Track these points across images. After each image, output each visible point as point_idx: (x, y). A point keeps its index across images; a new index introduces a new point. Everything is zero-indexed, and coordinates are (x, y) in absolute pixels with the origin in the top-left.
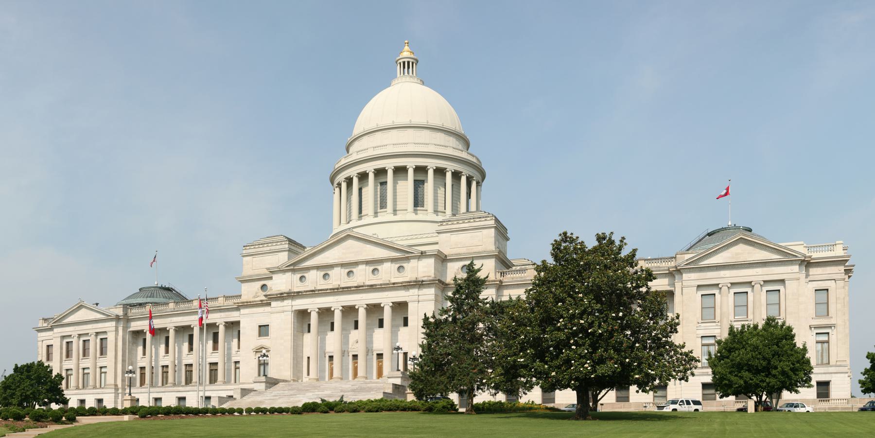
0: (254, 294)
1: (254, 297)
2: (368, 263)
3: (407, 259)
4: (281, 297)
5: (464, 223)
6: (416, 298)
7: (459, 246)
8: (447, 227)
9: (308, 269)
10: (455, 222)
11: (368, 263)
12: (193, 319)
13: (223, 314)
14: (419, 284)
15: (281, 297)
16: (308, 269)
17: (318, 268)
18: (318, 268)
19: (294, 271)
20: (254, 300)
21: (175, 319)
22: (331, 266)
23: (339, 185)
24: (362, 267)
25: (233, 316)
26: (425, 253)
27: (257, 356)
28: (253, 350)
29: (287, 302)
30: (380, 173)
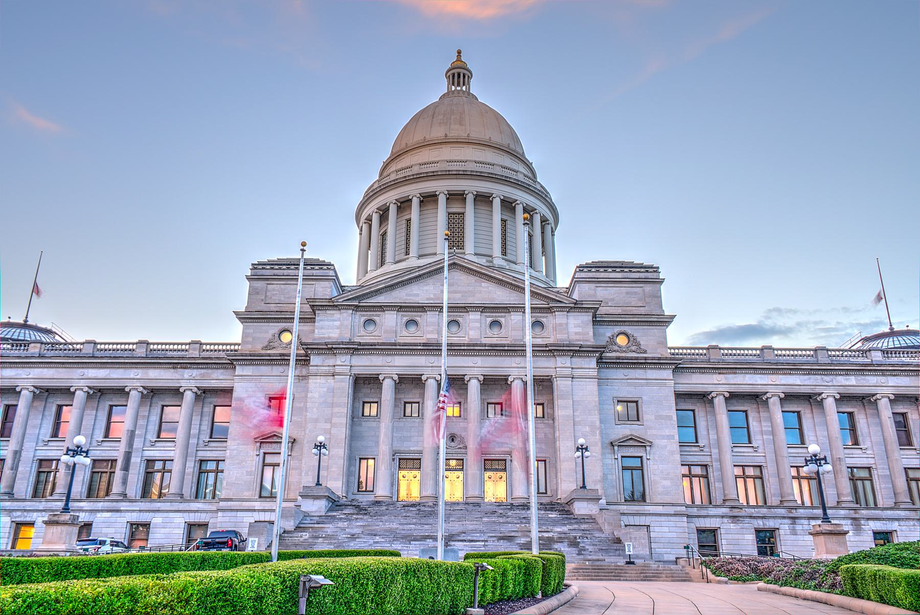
0: (267, 343)
1: (266, 348)
2: (484, 309)
3: (549, 310)
4: (330, 349)
5: (614, 271)
6: (568, 372)
7: (610, 305)
8: (590, 275)
9: (382, 308)
10: (602, 270)
11: (484, 309)
12: (132, 376)
13: (195, 373)
14: (576, 351)
15: (330, 349)
16: (382, 308)
17: (400, 308)
18: (400, 308)
19: (357, 308)
20: (264, 352)
21: (92, 373)
22: (422, 308)
23: (369, 219)
24: (474, 316)
25: (217, 379)
26: (582, 304)
27: (262, 451)
28: (255, 439)
29: (342, 360)
30: (456, 197)
